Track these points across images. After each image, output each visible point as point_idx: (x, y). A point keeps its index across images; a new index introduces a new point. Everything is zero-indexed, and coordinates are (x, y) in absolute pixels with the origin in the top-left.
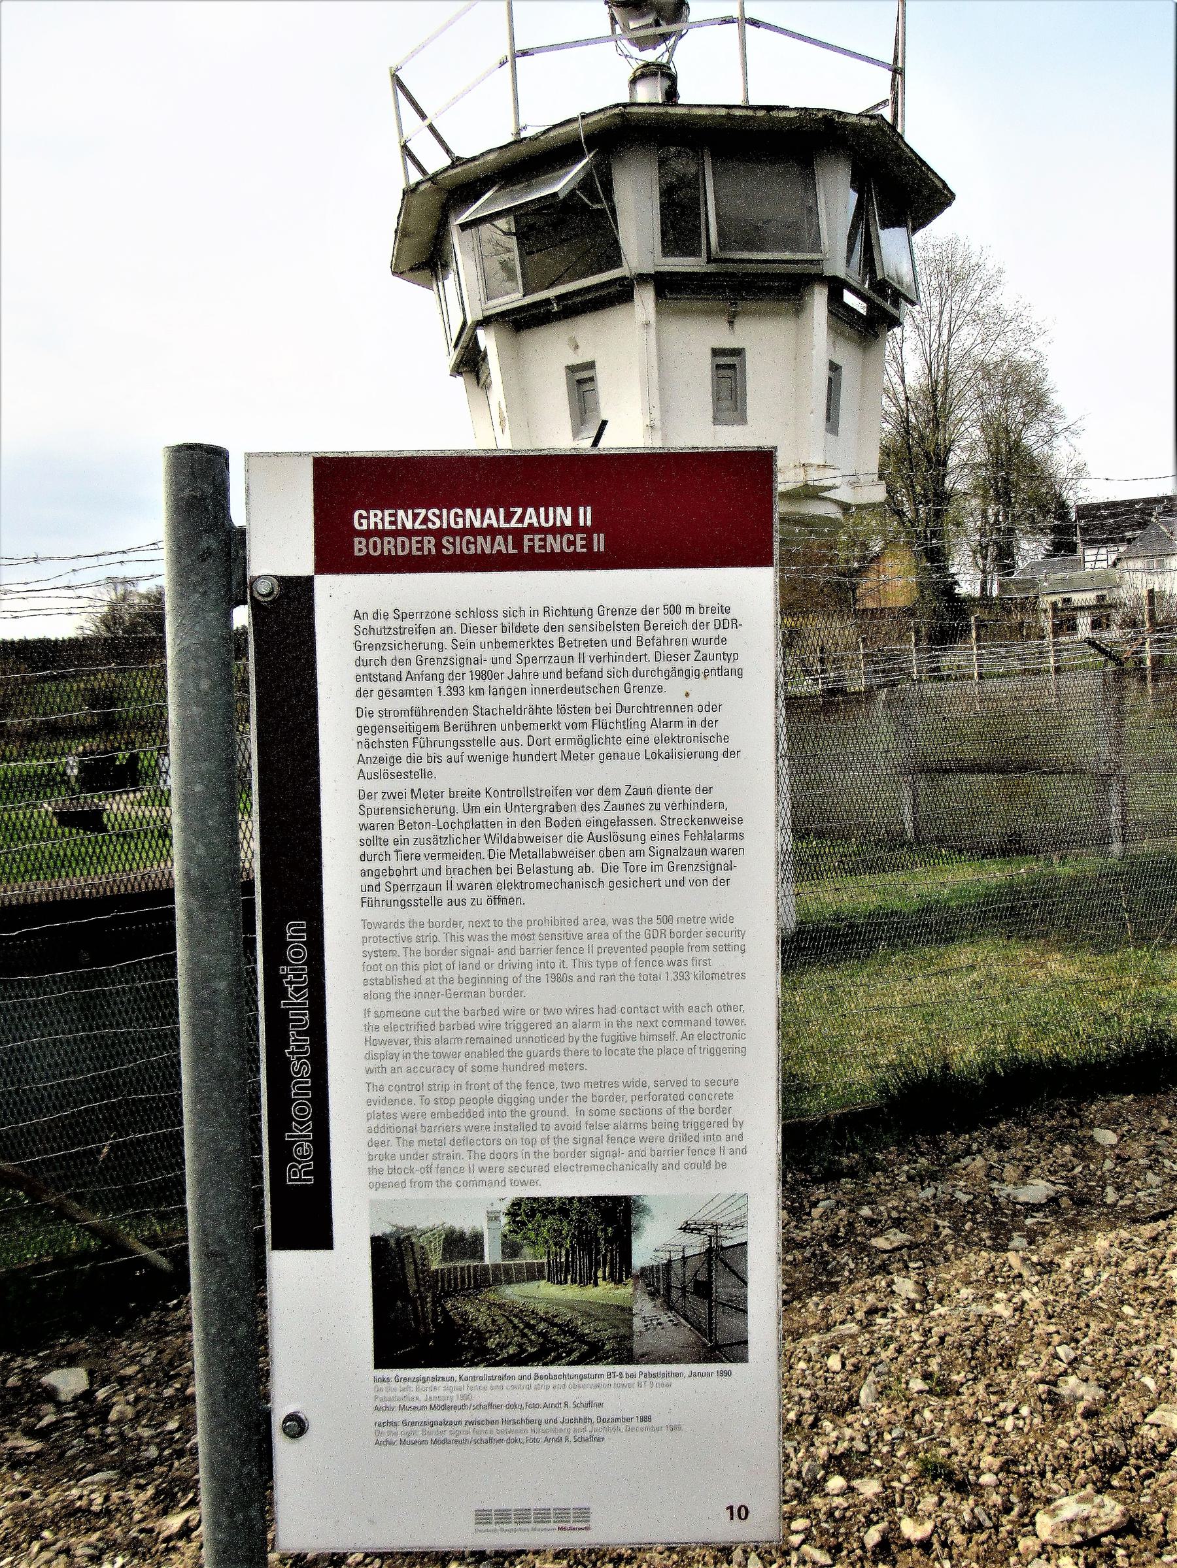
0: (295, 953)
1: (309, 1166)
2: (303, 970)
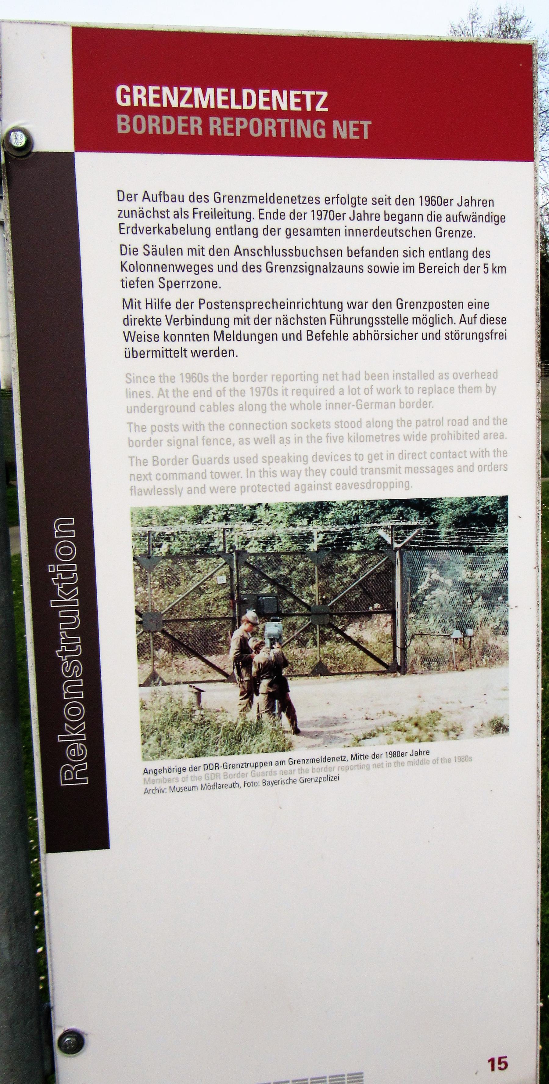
1: (84, 767)
2: (73, 568)
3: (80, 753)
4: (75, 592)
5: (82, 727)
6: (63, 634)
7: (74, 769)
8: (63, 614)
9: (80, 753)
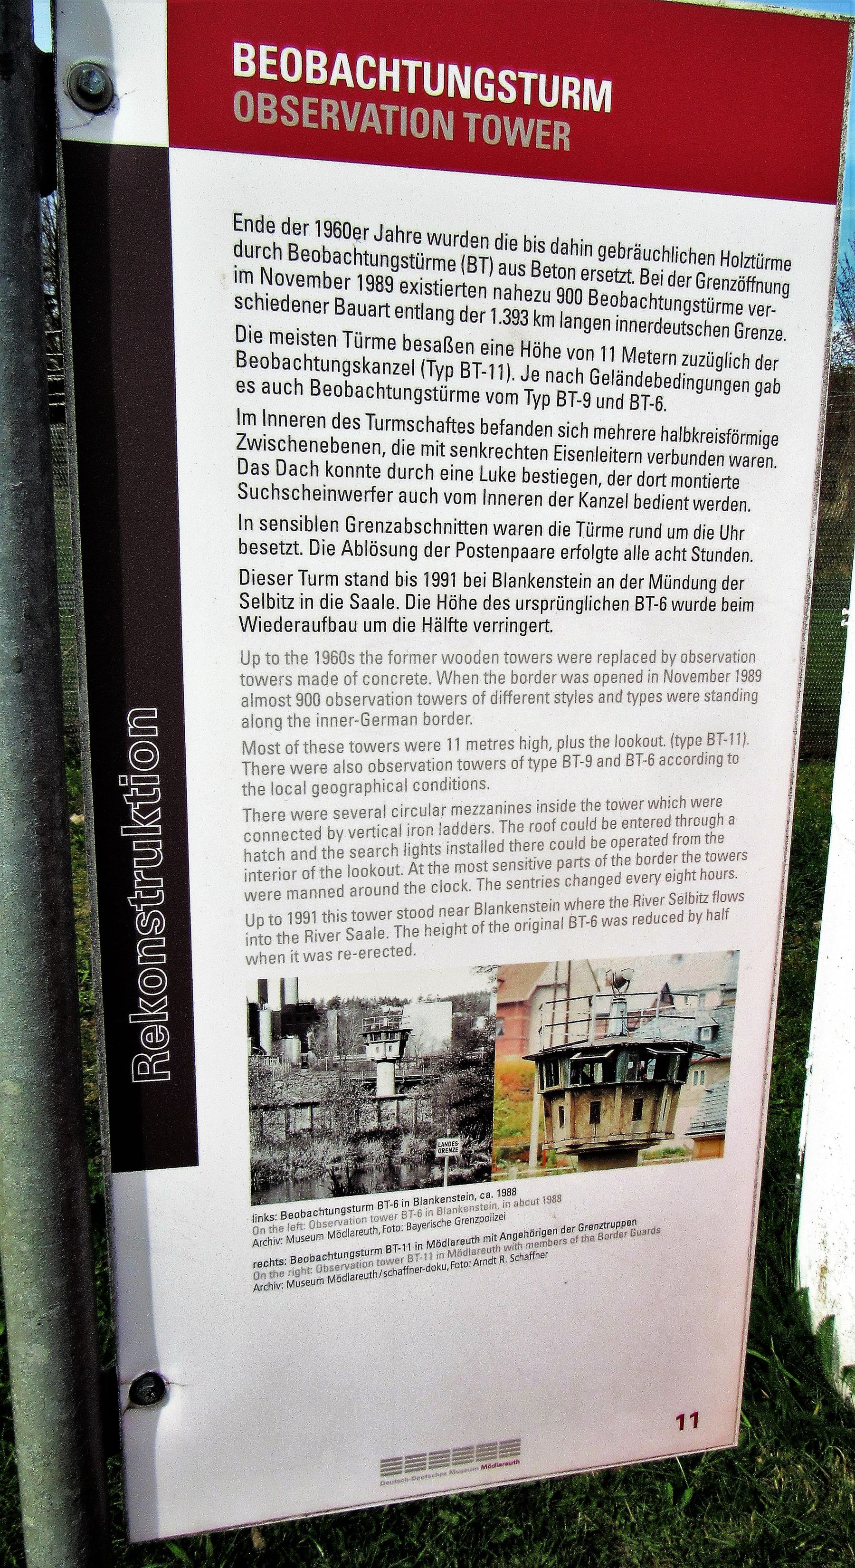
0: (146, 756)
1: (165, 1057)
2: (155, 780)
3: (160, 1037)
4: (156, 815)
5: (163, 1003)
6: (139, 875)
7: (150, 1060)
8: (138, 846)
9: (160, 1037)
